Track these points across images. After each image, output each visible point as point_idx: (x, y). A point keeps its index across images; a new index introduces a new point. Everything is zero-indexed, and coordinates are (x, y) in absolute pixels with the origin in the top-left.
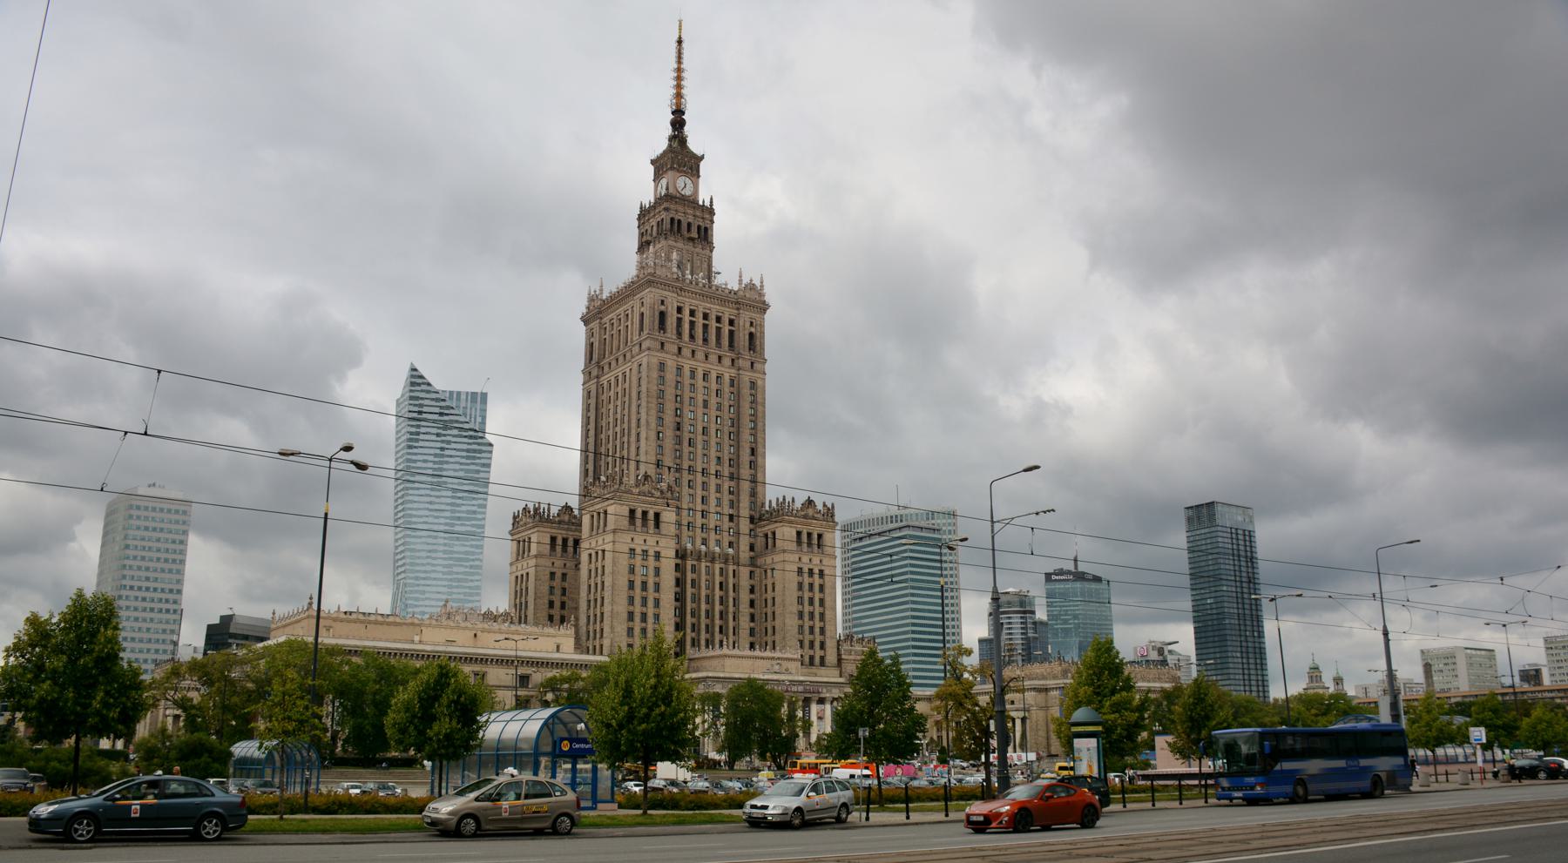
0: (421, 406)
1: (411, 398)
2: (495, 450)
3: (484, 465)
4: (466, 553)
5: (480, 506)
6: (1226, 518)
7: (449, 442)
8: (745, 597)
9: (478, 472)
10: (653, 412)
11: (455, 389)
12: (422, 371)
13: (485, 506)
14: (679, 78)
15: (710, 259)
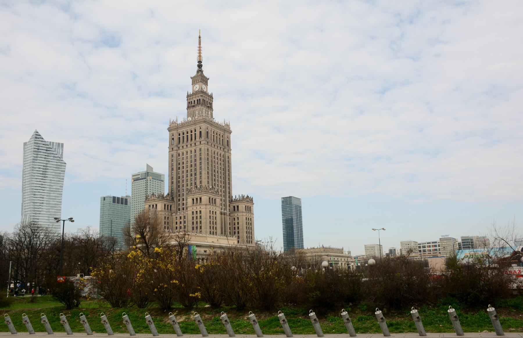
0: (39, 146)
1: (35, 143)
2: (67, 165)
3: (62, 171)
4: (55, 204)
5: (60, 186)
6: (294, 202)
7: (49, 161)
8: (228, 226)
9: (60, 173)
10: (206, 165)
11: (52, 141)
12: (40, 133)
13: (62, 187)
14: (200, 50)
15: (212, 114)
